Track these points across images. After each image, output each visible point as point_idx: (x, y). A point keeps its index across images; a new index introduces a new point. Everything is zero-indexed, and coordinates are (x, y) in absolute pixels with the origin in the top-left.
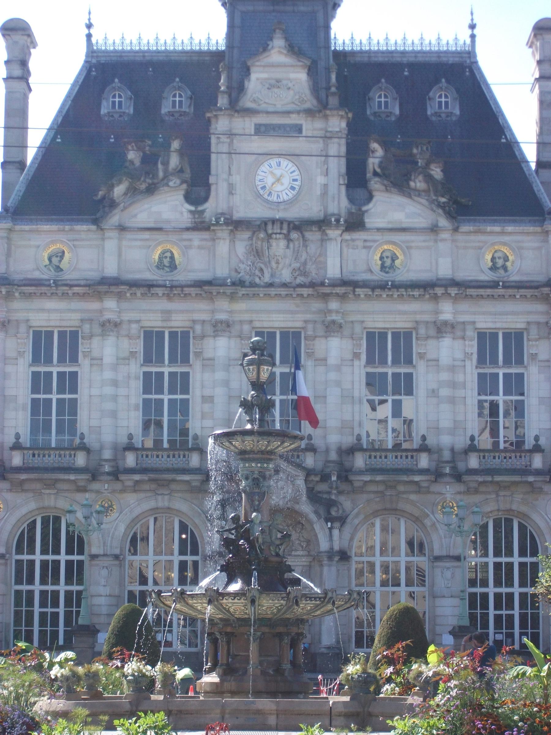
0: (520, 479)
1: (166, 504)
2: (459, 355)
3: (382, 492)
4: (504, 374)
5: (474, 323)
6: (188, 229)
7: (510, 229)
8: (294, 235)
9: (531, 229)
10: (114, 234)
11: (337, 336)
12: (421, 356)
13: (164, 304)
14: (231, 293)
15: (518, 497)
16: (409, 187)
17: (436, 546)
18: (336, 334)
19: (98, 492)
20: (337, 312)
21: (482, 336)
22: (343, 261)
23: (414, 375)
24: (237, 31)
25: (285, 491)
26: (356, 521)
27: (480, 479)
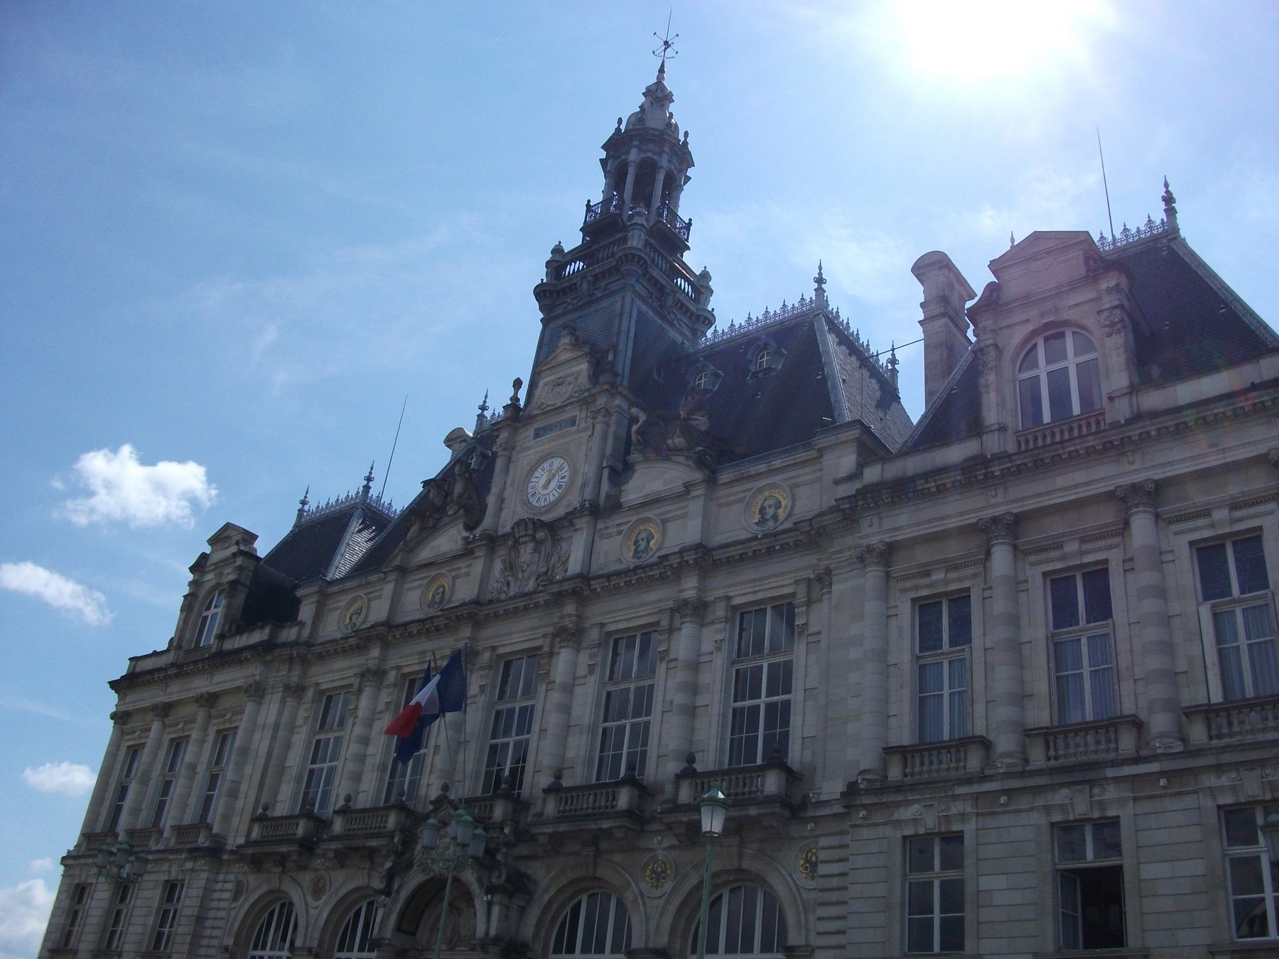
2: (707, 646)
5: (728, 598)
6: (461, 556)
7: (777, 463)
8: (540, 535)
9: (801, 456)
17: (635, 934)
19: (316, 870)
20: (570, 615)
24: (545, 349)
26: (546, 898)
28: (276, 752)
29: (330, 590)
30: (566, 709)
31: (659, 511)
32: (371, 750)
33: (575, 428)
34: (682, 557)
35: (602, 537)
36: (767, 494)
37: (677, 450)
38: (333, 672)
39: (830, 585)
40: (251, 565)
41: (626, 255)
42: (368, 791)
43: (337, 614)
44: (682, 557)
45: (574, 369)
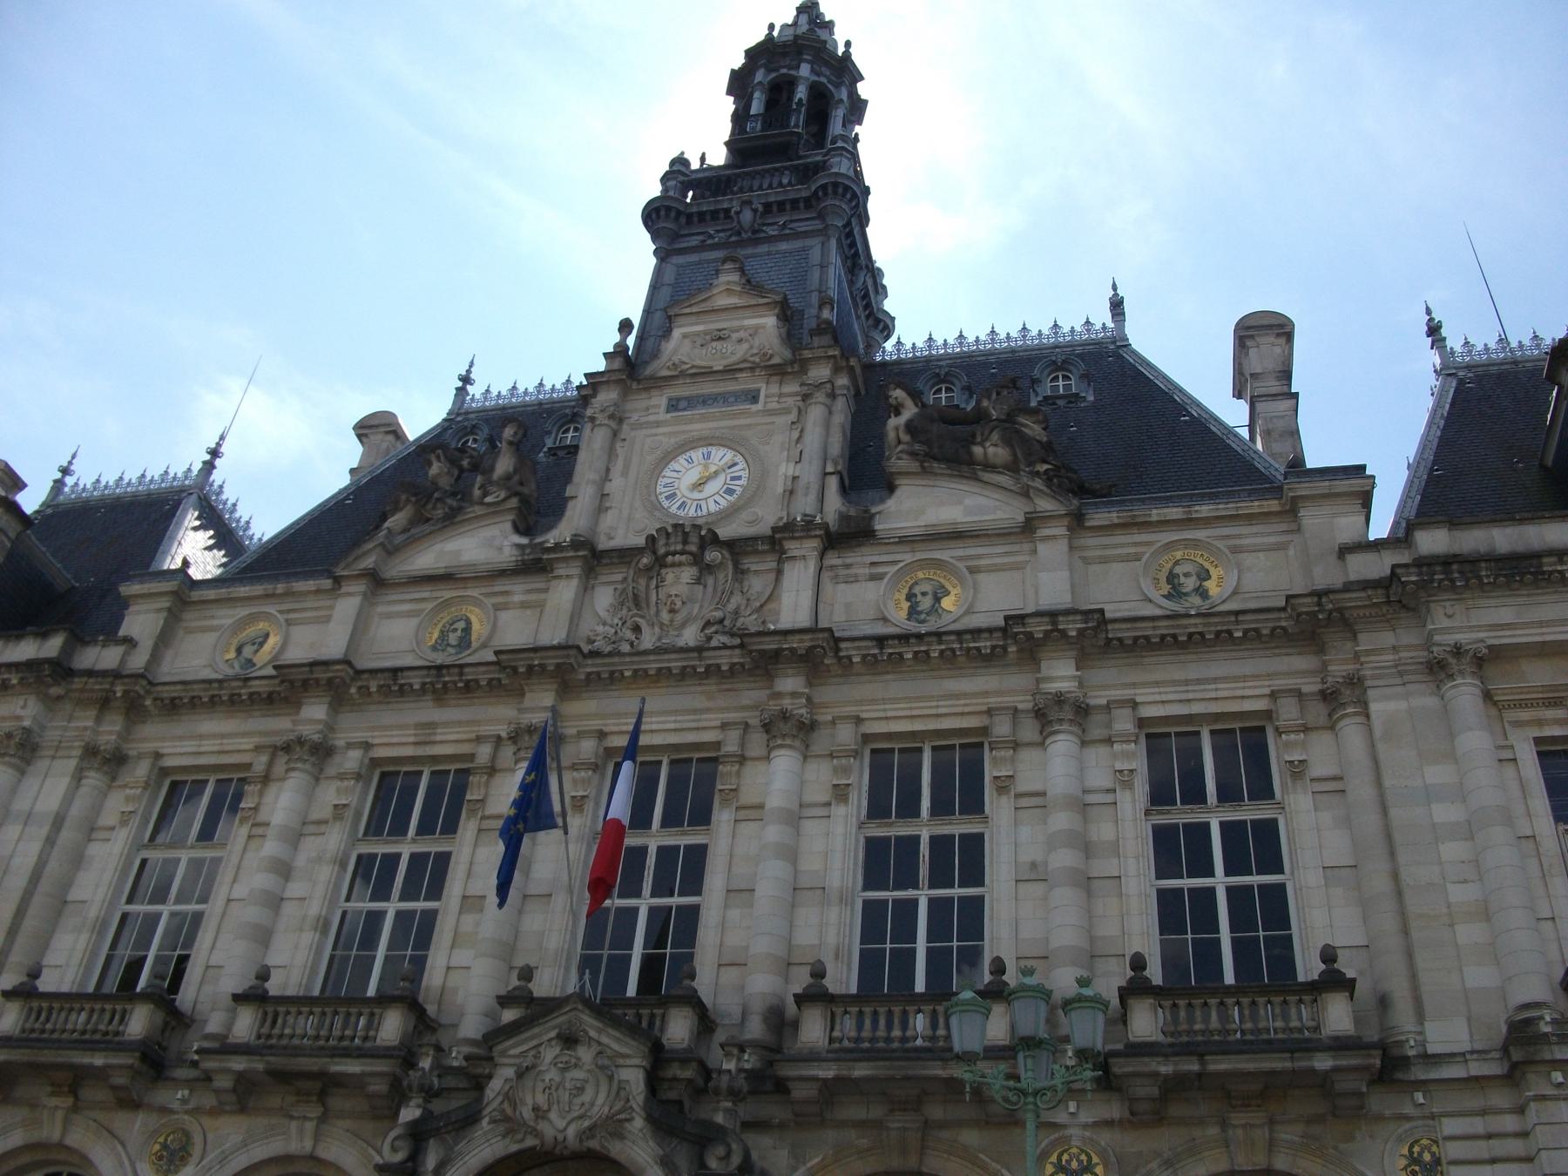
0: (1288, 1065)
1: (308, 1145)
2: (1099, 778)
3: (878, 1125)
4: (1224, 826)
7: (1204, 510)
8: (713, 555)
10: (359, 587)
11: (790, 747)
12: (1003, 785)
13: (427, 712)
14: (558, 666)
15: (1289, 1134)
16: (971, 462)
18: (788, 742)
19: (164, 1110)
20: (794, 695)
21: (1155, 737)
22: (821, 606)
23: (986, 838)
24: (665, 292)
25: (587, 1097)
27: (1165, 1069)
28: (53, 867)
29: (196, 595)
30: (791, 854)
31: (960, 553)
32: (295, 889)
33: (754, 408)
34: (1054, 623)
35: (836, 580)
36: (1179, 555)
37: (990, 467)
38: (201, 737)
39: (1364, 704)
40: (13, 528)
41: (836, 185)
42: (296, 963)
43: (210, 638)
44: (1054, 623)
45: (747, 322)
